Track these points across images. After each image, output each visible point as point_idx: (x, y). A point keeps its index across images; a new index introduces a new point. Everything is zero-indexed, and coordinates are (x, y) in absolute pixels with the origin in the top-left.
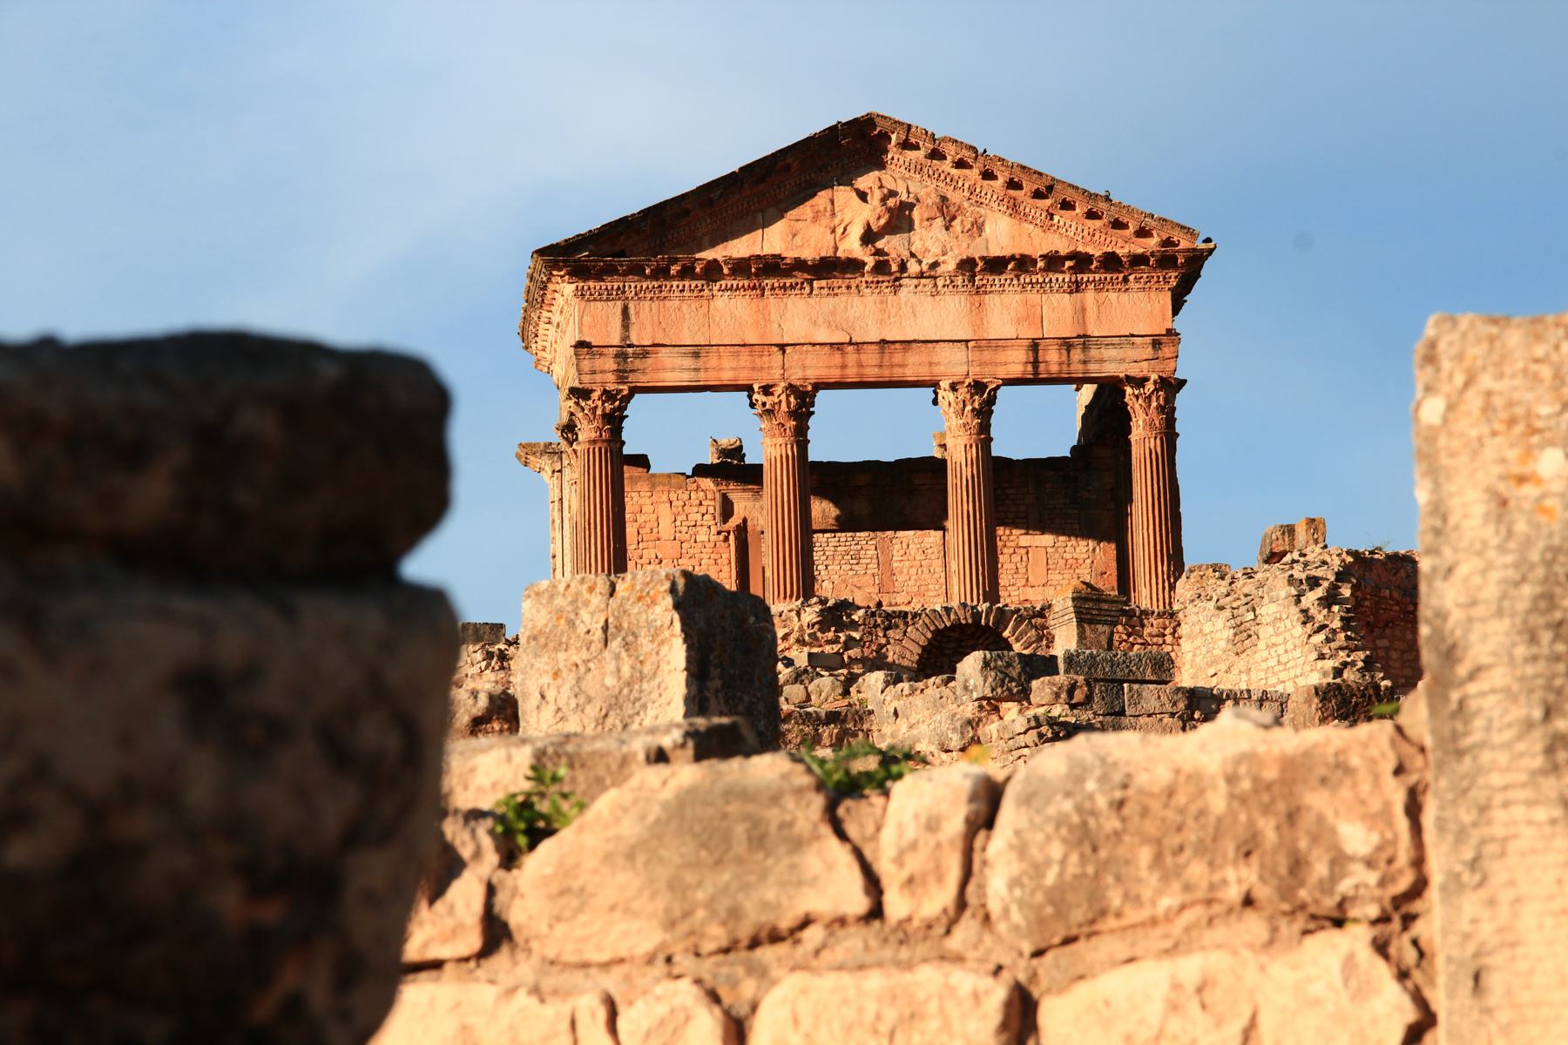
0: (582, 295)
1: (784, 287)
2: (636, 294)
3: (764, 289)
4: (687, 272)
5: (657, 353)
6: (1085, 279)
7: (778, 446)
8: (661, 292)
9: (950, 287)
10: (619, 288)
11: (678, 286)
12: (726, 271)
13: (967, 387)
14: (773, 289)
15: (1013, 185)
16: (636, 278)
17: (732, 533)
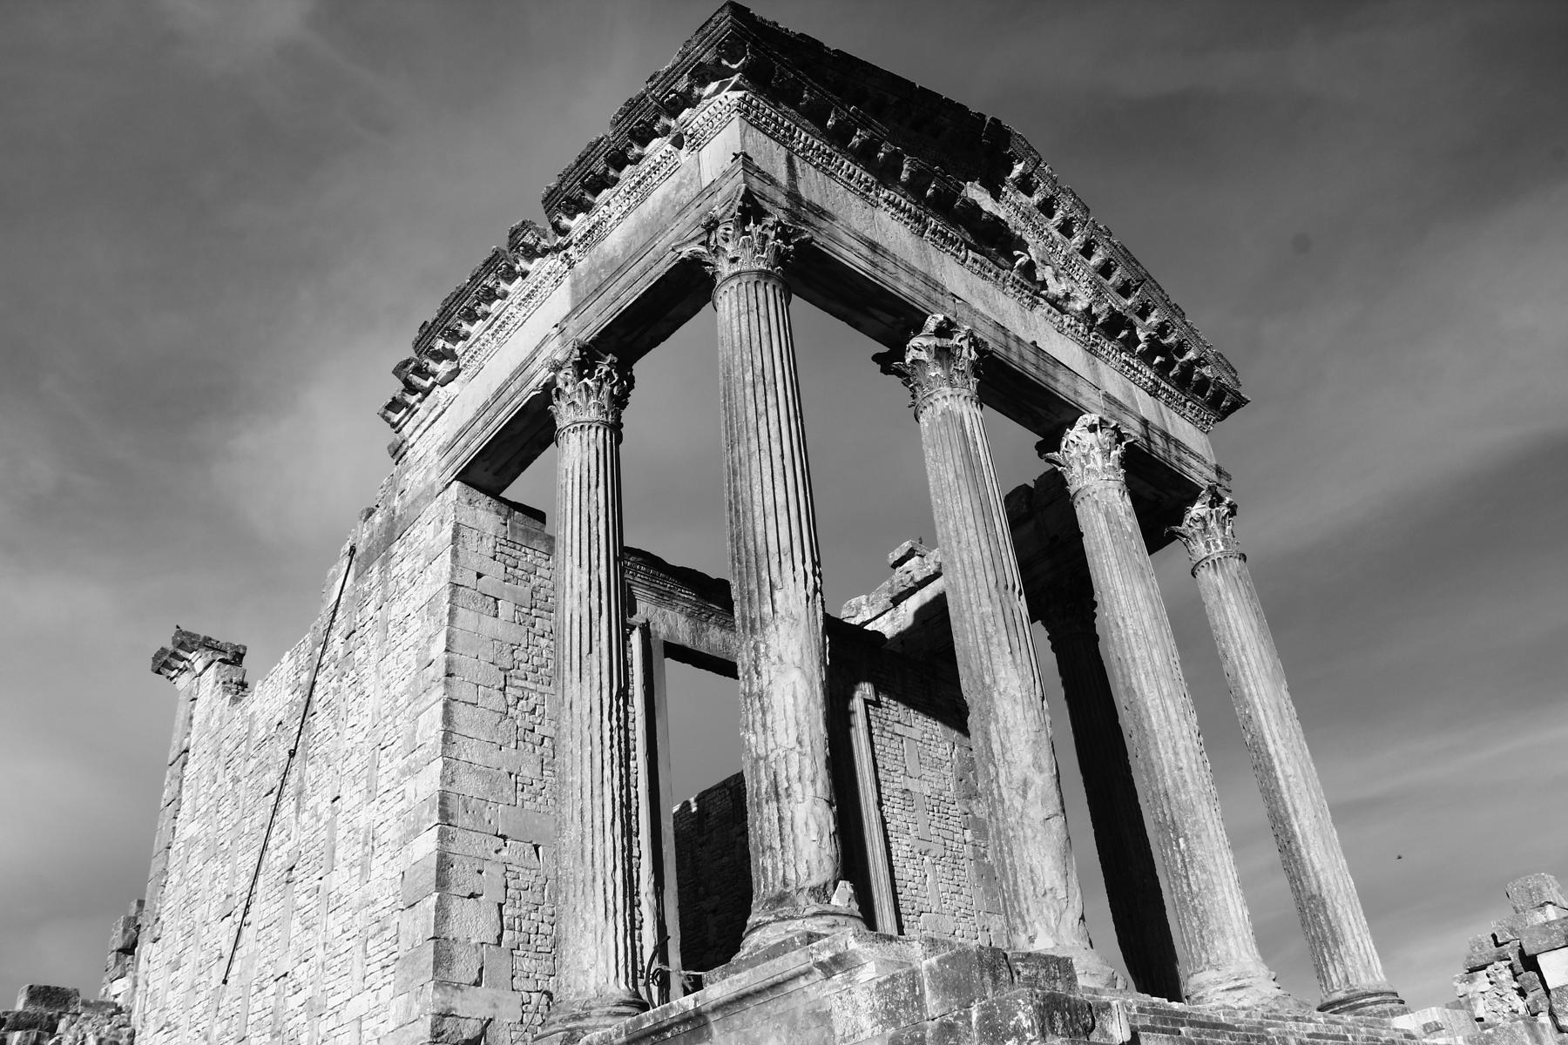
0: (747, 110)
1: (944, 235)
2: (803, 149)
3: (925, 227)
4: (864, 155)
5: (833, 220)
6: (1162, 385)
7: (961, 398)
8: (829, 164)
9: (1073, 330)
10: (788, 129)
11: (848, 167)
12: (904, 176)
13: (1112, 429)
14: (934, 232)
15: (1106, 270)
16: (812, 127)
17: (637, 629)
